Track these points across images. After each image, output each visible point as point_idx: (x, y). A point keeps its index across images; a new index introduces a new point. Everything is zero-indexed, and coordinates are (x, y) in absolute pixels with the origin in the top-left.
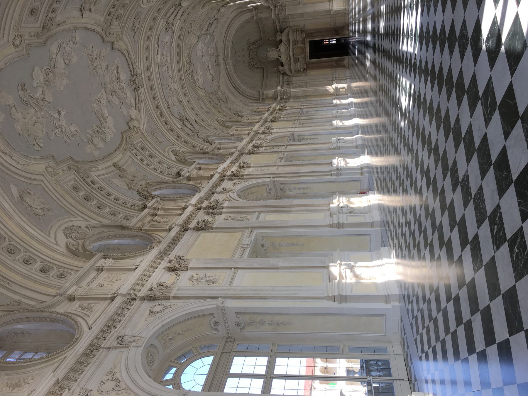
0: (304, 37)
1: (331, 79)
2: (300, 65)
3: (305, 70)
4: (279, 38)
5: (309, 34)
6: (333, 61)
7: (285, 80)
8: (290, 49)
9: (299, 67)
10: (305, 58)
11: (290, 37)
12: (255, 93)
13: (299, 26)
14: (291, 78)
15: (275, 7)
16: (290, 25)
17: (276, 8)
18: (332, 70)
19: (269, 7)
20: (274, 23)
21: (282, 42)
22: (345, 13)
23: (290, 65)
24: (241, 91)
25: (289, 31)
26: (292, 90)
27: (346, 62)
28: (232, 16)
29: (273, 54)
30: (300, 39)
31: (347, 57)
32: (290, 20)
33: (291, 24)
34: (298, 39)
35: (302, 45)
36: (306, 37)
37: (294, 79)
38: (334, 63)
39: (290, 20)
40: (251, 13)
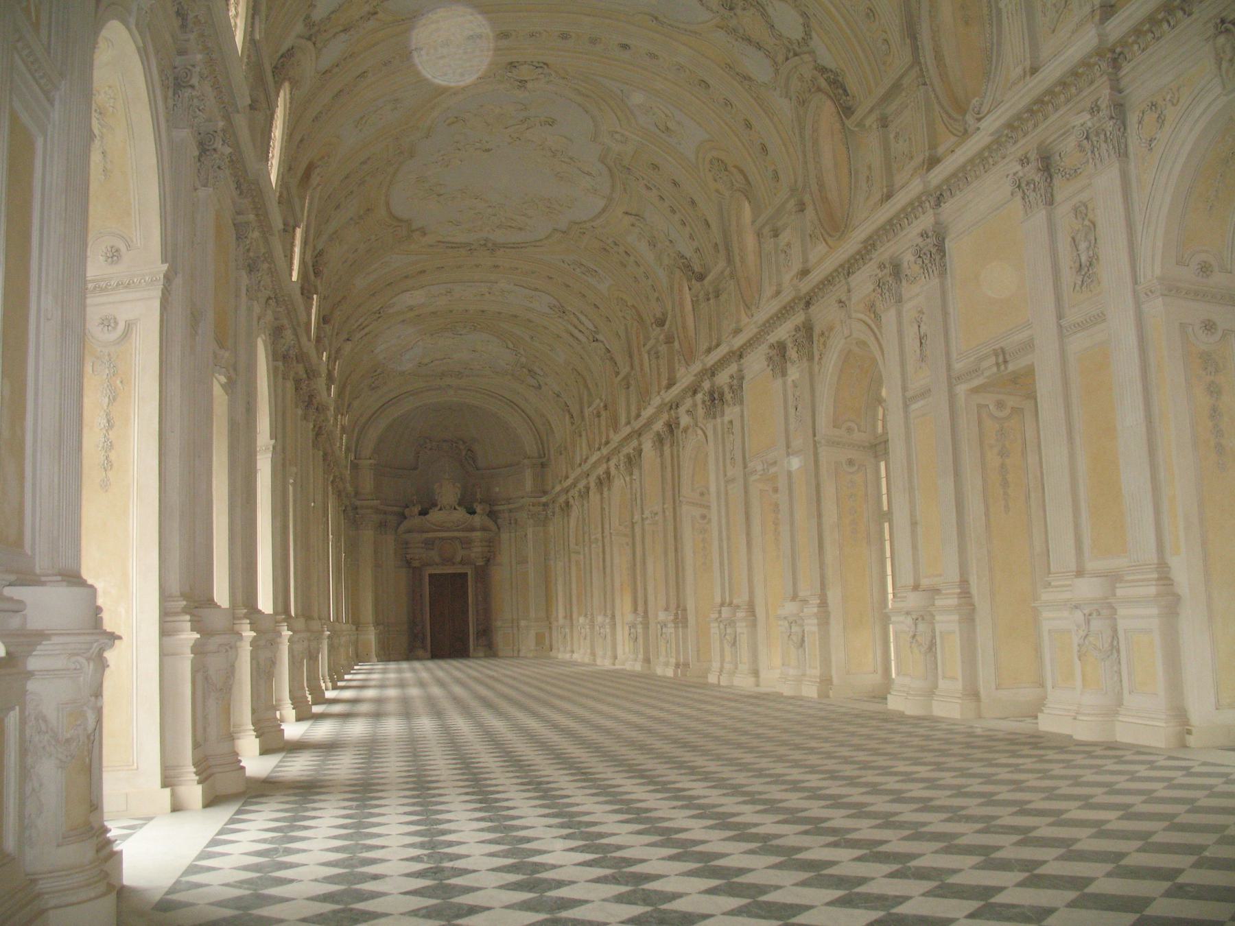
0: (478, 564)
5: (483, 574)
8: (454, 531)
11: (478, 534)
21: (470, 513)
29: (448, 493)
30: (473, 555)
33: (504, 536)
34: (475, 550)
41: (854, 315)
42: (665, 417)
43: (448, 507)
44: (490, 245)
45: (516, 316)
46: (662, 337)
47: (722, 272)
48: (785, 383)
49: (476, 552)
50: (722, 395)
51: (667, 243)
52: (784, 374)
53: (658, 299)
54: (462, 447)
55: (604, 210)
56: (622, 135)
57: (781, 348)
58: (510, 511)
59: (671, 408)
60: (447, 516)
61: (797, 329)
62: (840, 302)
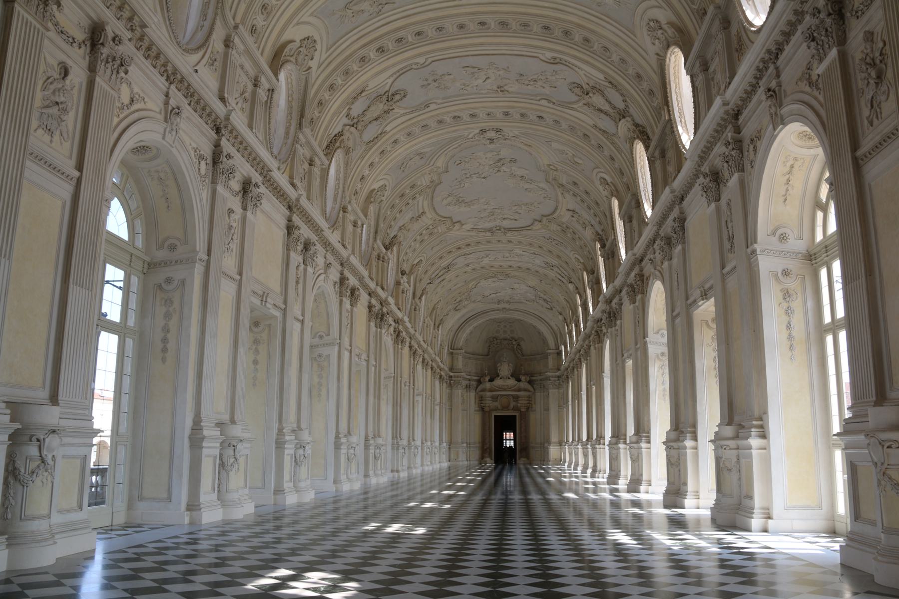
1: (468, 441)
2: (489, 403)
3: (482, 409)
4: (523, 378)
5: (525, 416)
6: (490, 445)
7: (472, 383)
9: (487, 402)
10: (496, 409)
12: (461, 344)
13: (535, 404)
14: (474, 391)
15: (559, 377)
16: (536, 394)
17: (557, 379)
18: (479, 443)
19: (559, 370)
20: (541, 373)
22: (544, 461)
23: (490, 391)
24: (464, 326)
25: (529, 391)
26: (460, 391)
27: (488, 460)
28: (553, 324)
29: (505, 369)
30: (519, 405)
31: (493, 461)
32: (542, 393)
33: (538, 394)
34: (520, 402)
35: (512, 406)
36: (521, 412)
37: (473, 394)
38: (488, 446)
39: (542, 393)
40: (554, 348)
41: (658, 268)
42: (595, 326)
43: (505, 377)
44: (502, 230)
45: (528, 269)
46: (594, 280)
47: (612, 243)
48: (634, 307)
49: (522, 402)
50: (615, 314)
51: (590, 227)
52: (634, 302)
53: (592, 259)
54: (514, 343)
55: (556, 209)
56: (554, 167)
57: (631, 286)
58: (541, 380)
59: (598, 321)
60: (505, 382)
61: (635, 276)
62: (651, 260)
